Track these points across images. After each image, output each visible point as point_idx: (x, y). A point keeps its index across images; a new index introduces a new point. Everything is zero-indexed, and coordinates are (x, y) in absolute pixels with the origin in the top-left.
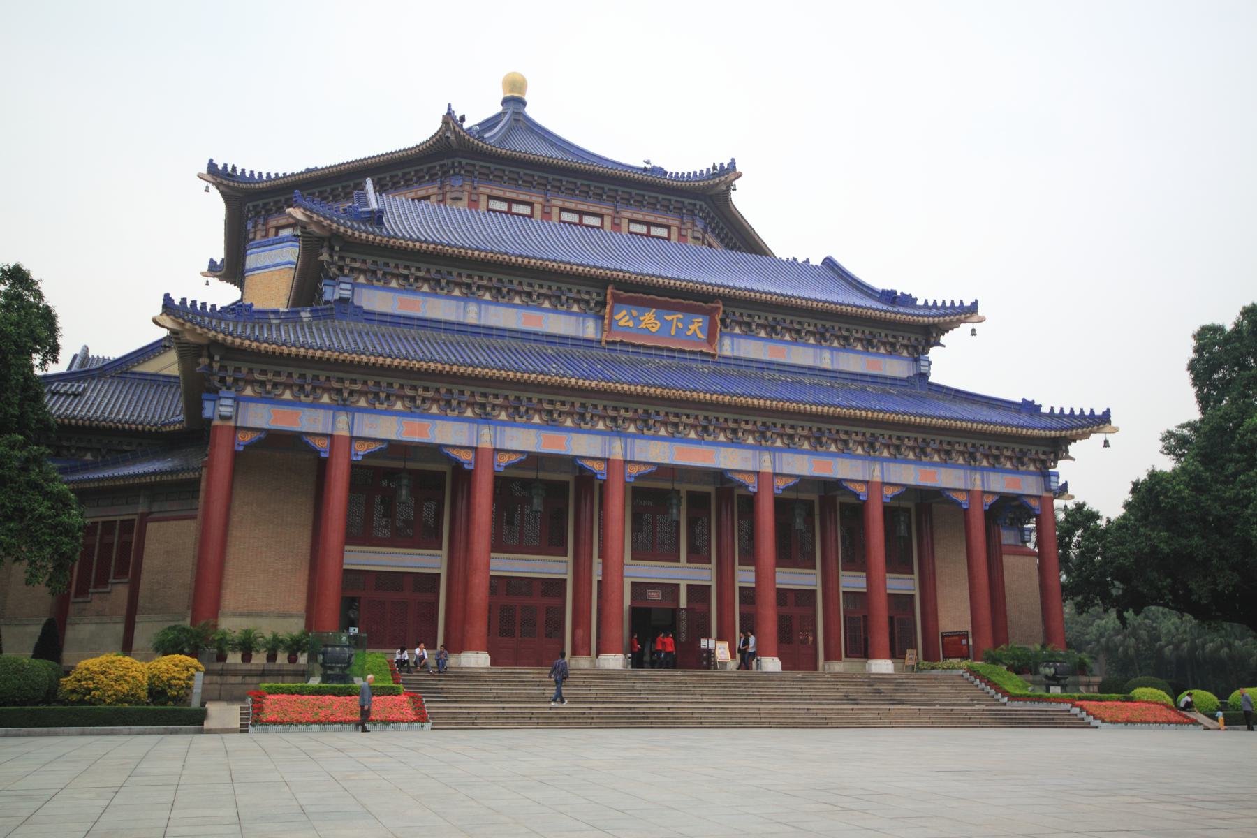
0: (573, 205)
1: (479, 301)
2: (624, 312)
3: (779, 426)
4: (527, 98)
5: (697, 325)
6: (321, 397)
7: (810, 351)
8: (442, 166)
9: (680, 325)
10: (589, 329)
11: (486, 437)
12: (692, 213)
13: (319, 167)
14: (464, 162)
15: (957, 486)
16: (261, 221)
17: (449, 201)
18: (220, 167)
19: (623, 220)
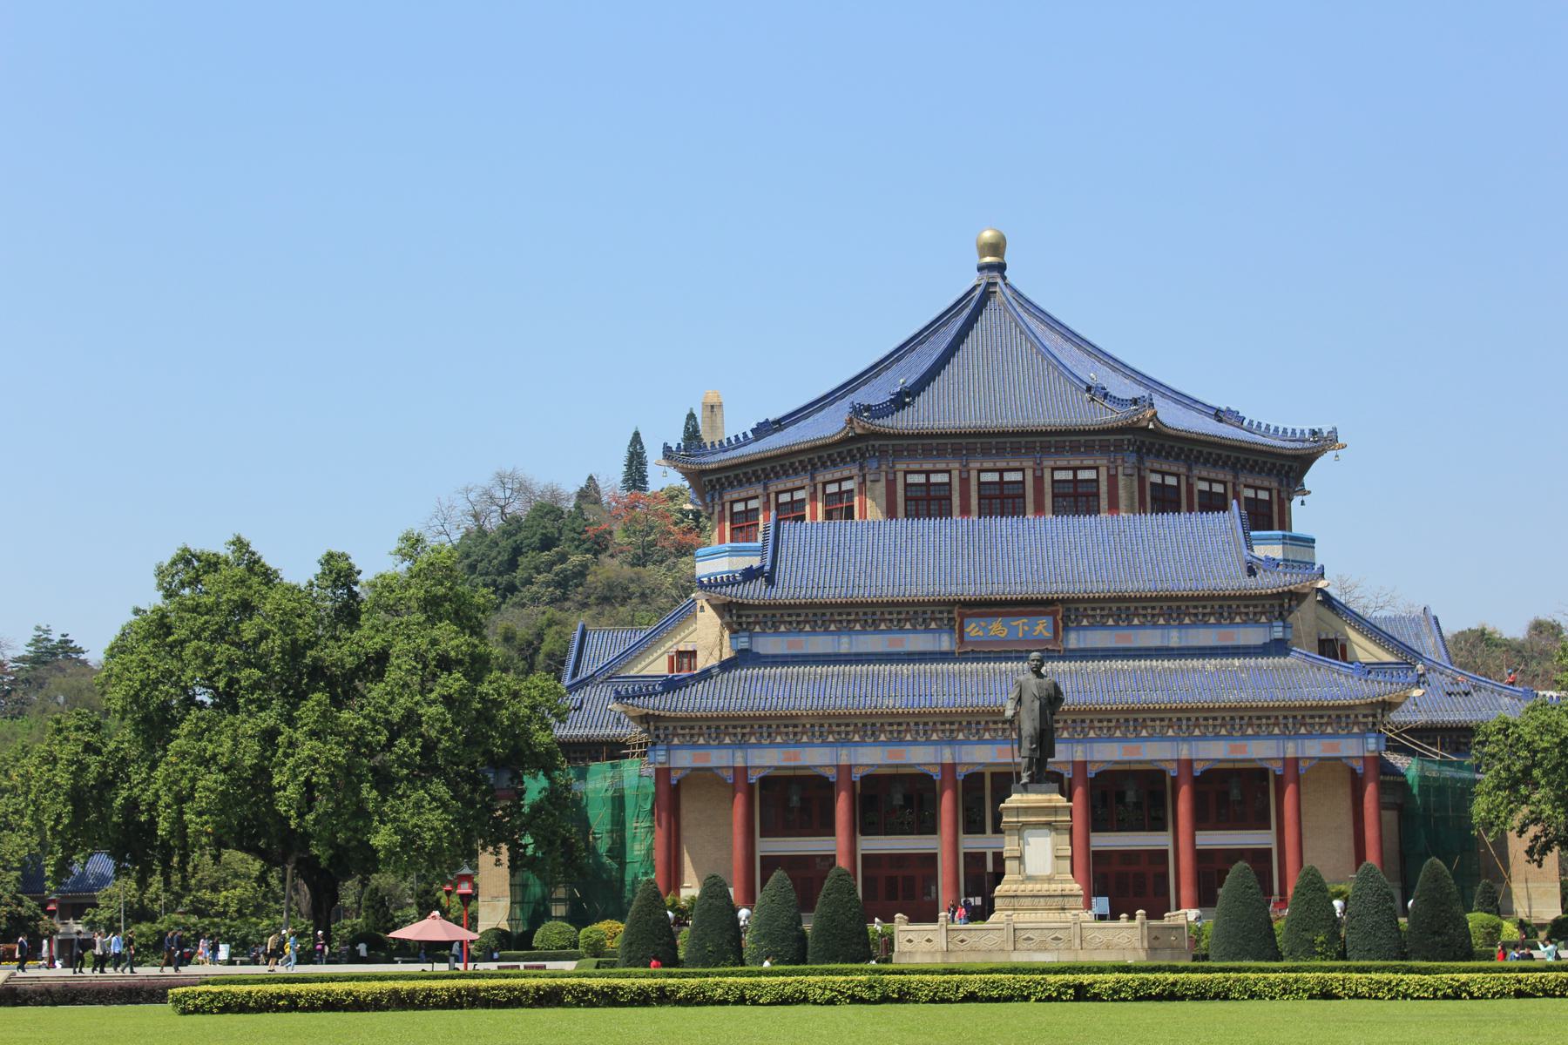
0: (992, 464)
1: (851, 631)
2: (973, 625)
3: (1088, 721)
4: (1008, 259)
5: (1042, 627)
6: (724, 740)
7: (1158, 632)
8: (859, 449)
9: (1026, 628)
10: (945, 643)
11: (845, 756)
12: (1119, 447)
13: (771, 419)
14: (877, 443)
15: (1270, 756)
16: (717, 496)
17: (868, 483)
18: (674, 449)
19: (1045, 470)
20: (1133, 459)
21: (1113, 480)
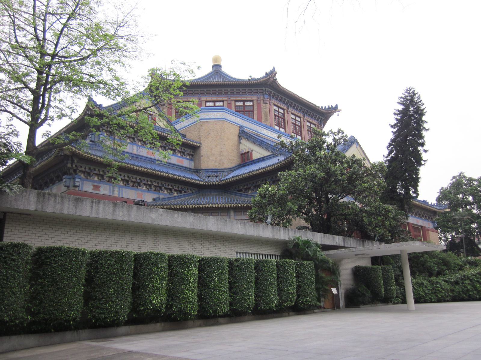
4: (222, 64)
20: (266, 97)
21: (259, 104)
